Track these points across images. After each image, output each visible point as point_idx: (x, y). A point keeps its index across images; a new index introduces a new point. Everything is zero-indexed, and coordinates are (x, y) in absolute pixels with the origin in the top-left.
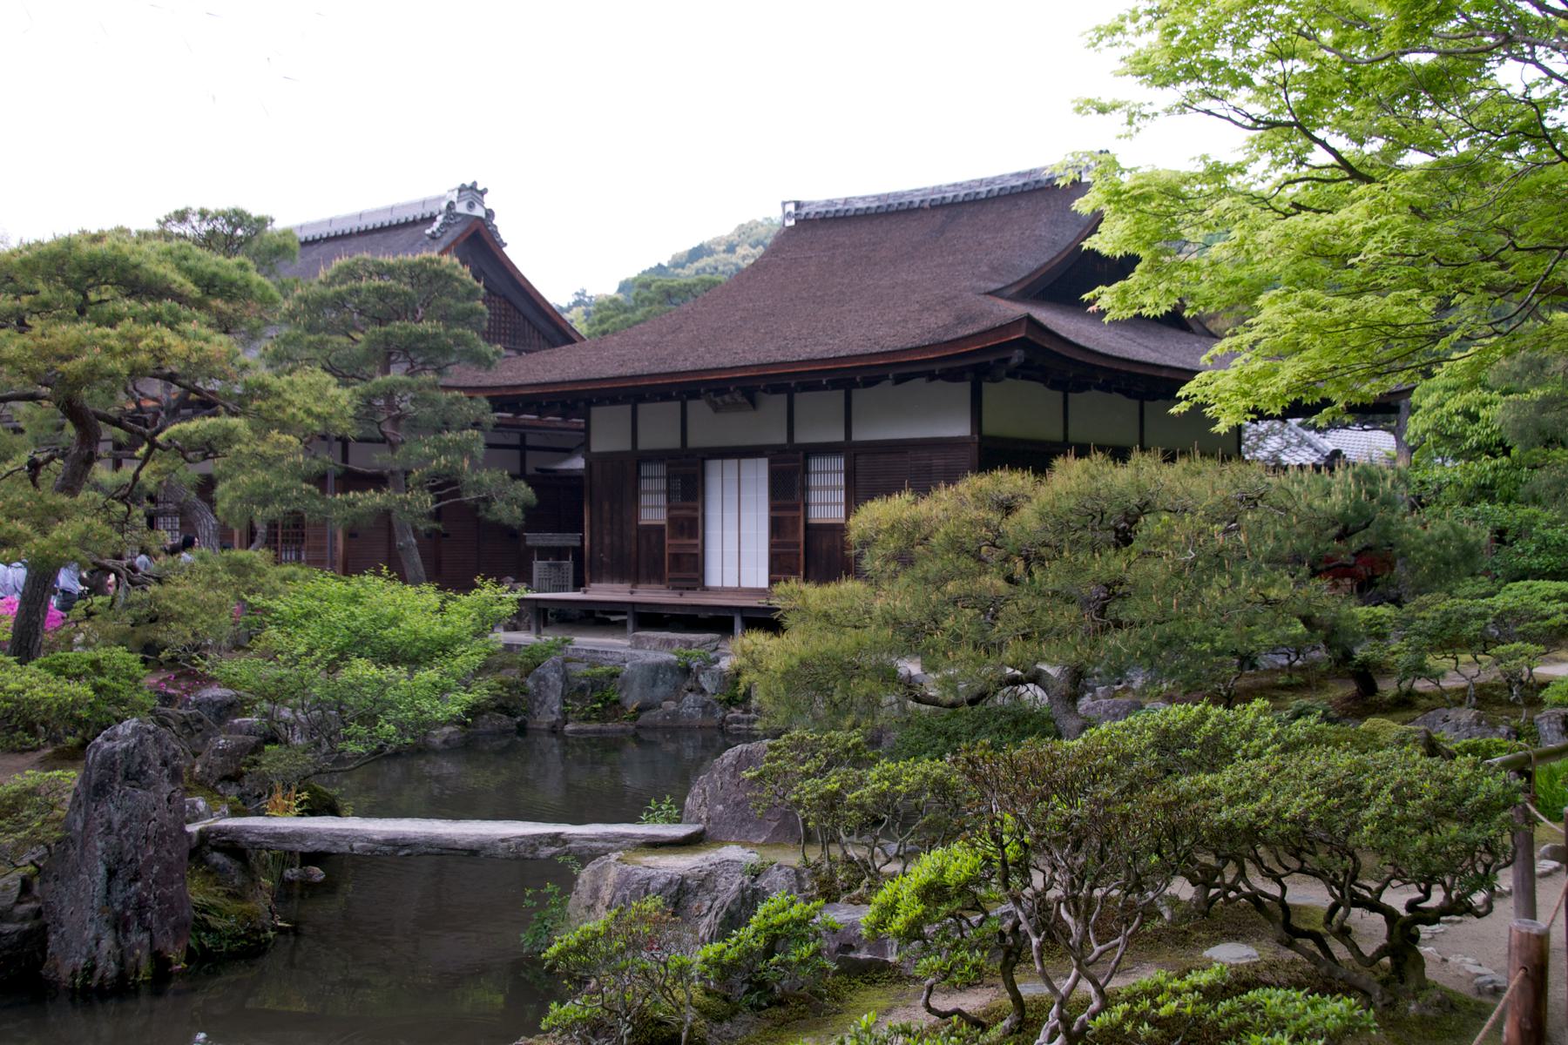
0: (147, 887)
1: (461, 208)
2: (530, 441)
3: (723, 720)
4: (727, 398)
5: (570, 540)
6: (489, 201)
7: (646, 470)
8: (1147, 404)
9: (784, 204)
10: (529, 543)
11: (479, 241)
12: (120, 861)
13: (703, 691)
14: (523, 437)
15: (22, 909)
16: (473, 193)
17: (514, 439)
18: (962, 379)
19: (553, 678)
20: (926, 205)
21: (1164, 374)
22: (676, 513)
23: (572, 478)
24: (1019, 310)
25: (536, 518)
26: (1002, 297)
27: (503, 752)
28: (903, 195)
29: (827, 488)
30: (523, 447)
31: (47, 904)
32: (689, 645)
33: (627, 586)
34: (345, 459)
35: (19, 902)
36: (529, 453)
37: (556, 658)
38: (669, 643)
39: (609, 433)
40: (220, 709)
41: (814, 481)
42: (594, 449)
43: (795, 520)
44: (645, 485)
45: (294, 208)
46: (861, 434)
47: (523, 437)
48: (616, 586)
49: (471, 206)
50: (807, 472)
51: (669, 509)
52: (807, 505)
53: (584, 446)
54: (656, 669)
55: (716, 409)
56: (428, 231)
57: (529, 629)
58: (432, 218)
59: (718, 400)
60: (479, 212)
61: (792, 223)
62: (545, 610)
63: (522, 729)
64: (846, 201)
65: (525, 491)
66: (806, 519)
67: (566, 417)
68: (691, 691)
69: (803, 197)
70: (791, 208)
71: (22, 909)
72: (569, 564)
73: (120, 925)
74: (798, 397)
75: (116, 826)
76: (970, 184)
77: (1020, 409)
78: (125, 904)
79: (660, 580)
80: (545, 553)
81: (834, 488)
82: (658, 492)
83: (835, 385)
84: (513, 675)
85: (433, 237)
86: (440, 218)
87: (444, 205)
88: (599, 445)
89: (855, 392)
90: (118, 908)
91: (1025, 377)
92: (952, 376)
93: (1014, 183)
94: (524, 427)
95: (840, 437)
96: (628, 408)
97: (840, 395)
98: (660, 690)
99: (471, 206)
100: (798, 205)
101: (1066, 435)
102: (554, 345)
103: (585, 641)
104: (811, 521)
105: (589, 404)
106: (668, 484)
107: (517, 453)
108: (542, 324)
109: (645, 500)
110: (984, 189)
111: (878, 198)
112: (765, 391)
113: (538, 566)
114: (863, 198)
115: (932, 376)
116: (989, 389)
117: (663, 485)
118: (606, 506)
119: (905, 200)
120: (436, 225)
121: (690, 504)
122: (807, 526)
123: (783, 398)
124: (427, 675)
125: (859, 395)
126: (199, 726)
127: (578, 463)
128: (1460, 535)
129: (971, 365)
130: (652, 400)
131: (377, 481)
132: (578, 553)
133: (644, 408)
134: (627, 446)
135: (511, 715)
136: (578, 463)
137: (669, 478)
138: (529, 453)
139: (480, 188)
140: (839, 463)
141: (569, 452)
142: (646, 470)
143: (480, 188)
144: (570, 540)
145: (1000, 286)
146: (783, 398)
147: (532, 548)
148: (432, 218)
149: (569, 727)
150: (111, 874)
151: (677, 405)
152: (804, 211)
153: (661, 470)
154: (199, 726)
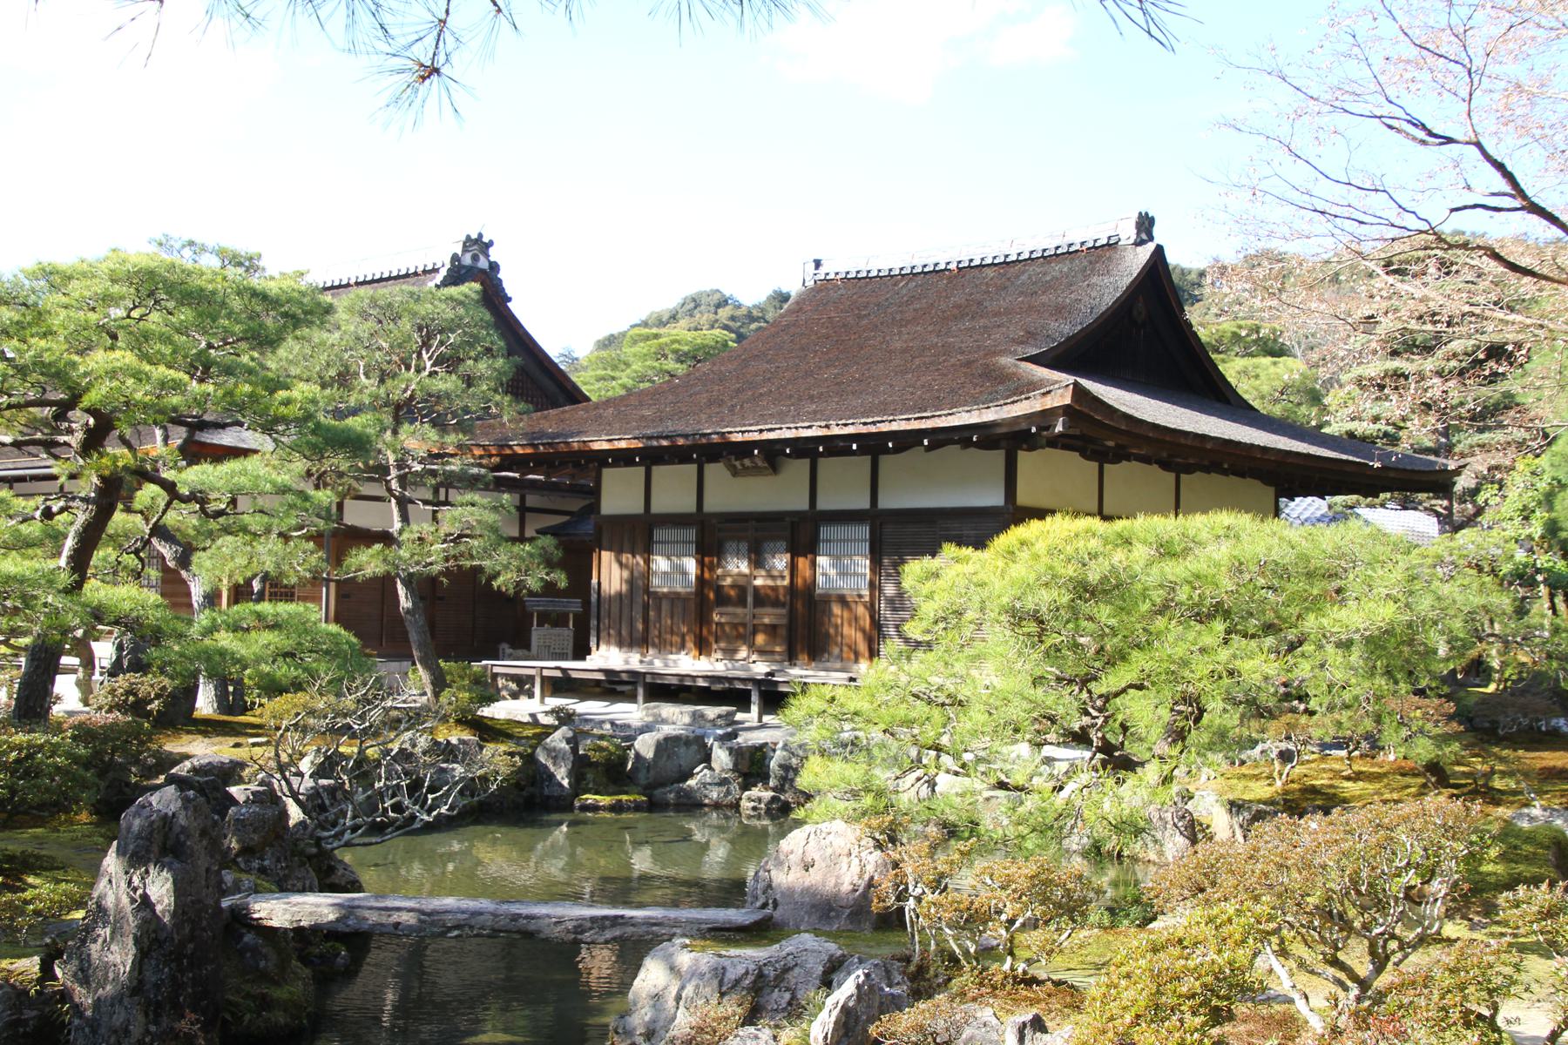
1: (467, 260)
4: (747, 462)
6: (494, 254)
20: (953, 266)
46: (887, 502)
55: (735, 473)
58: (435, 270)
59: (737, 463)
60: (483, 264)
74: (822, 462)
83: (862, 451)
86: (443, 272)
95: (864, 503)
99: (475, 258)
102: (555, 405)
108: (546, 382)
113: (537, 635)
115: (966, 443)
116: (1025, 459)
123: (806, 462)
125: (886, 462)
128: (1557, 680)
130: (615, 464)
133: (658, 471)
139: (485, 240)
140: (864, 531)
143: (485, 240)
146: (806, 462)
148: (435, 270)
151: (694, 467)
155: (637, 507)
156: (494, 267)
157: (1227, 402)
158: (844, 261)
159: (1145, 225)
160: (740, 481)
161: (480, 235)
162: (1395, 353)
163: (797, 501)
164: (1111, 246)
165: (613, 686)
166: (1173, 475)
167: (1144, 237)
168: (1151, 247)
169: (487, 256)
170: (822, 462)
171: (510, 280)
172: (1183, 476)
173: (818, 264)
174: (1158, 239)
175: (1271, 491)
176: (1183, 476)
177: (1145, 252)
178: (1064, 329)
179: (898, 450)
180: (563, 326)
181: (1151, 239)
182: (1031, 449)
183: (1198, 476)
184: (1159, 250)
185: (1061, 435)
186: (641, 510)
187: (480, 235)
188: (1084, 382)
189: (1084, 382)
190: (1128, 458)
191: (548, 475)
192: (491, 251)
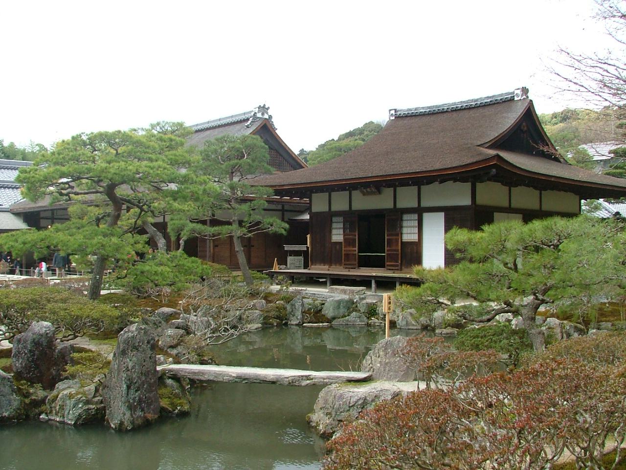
1: (259, 115)
2: (286, 208)
4: (368, 190)
5: (303, 248)
6: (270, 112)
7: (334, 219)
9: (390, 110)
10: (285, 249)
14: (283, 206)
16: (264, 109)
17: (280, 207)
20: (449, 110)
22: (347, 237)
26: (483, 147)
28: (440, 106)
30: (283, 211)
32: (353, 292)
33: (327, 267)
36: (285, 213)
38: (345, 292)
39: (319, 204)
40: (167, 316)
41: (405, 224)
43: (397, 241)
44: (334, 225)
45: (192, 119)
47: (283, 206)
48: (322, 267)
49: (263, 114)
50: (402, 220)
51: (344, 236)
52: (402, 234)
53: (308, 209)
55: (364, 195)
56: (246, 124)
58: (248, 119)
59: (365, 190)
60: (266, 116)
61: (394, 118)
62: (293, 277)
63: (286, 324)
64: (416, 109)
66: (401, 240)
67: (301, 198)
69: (398, 108)
70: (393, 112)
74: (398, 189)
76: (467, 102)
77: (491, 193)
79: (340, 264)
81: (413, 227)
82: (340, 228)
83: (414, 184)
85: (248, 127)
87: (252, 114)
88: (315, 209)
89: (422, 187)
94: (284, 202)
95: (416, 205)
97: (415, 189)
99: (263, 114)
100: (395, 110)
101: (510, 205)
104: (403, 241)
105: (312, 192)
106: (344, 225)
109: (334, 232)
110: (474, 103)
111: (429, 107)
112: (385, 187)
113: (290, 259)
114: (423, 108)
115: (455, 180)
117: (341, 225)
120: (250, 122)
121: (353, 233)
122: (402, 242)
126: (160, 325)
132: (305, 254)
133: (333, 194)
136: (307, 217)
139: (266, 107)
141: (302, 212)
142: (334, 219)
143: (266, 107)
148: (248, 119)
152: (398, 113)
153: (341, 219)
154: (160, 325)
155: (326, 209)
156: (270, 117)
163: (389, 205)
164: (512, 100)
166: (538, 192)
169: (267, 113)
172: (543, 192)
174: (530, 98)
175: (577, 197)
176: (543, 192)
179: (428, 183)
181: (528, 97)
183: (549, 191)
185: (493, 176)
188: (503, 154)
189: (503, 154)
191: (291, 198)
192: (269, 111)
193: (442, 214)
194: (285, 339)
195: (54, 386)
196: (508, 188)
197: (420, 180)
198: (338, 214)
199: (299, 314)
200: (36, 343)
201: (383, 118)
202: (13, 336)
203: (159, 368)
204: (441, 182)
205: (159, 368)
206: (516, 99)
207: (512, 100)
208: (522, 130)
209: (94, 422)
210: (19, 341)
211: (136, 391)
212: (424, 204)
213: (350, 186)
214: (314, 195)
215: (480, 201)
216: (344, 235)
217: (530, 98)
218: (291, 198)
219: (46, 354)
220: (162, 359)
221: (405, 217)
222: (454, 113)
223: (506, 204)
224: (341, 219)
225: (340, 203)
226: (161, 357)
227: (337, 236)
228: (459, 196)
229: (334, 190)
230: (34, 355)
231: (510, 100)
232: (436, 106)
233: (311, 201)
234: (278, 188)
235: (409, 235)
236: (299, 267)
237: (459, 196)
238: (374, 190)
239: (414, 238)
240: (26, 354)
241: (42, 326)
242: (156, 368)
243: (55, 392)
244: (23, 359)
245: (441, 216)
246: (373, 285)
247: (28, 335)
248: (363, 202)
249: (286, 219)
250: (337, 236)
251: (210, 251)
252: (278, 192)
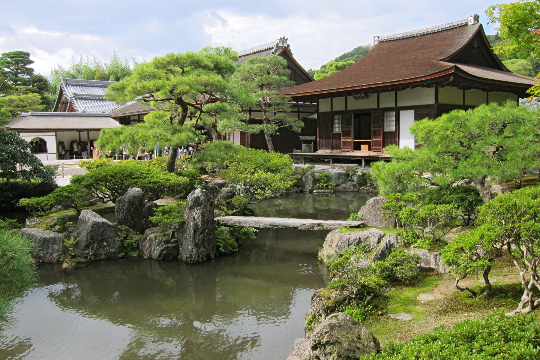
0: (204, 236)
1: (280, 44)
2: (301, 110)
3: (359, 189)
4: (359, 95)
5: (313, 138)
7: (335, 117)
8: (489, 93)
9: (375, 37)
11: (286, 53)
12: (197, 228)
13: (353, 181)
15: (172, 240)
16: (284, 40)
17: (296, 110)
18: (433, 87)
19: (310, 177)
21: (497, 83)
23: (314, 120)
24: (452, 65)
25: (305, 132)
27: (296, 198)
29: (390, 121)
30: (298, 112)
31: (179, 239)
34: (250, 116)
35: (172, 238)
36: (300, 114)
37: (310, 172)
39: (324, 106)
41: (386, 119)
42: (321, 110)
43: (380, 131)
44: (335, 121)
49: (283, 44)
50: (383, 116)
52: (383, 126)
53: (317, 111)
54: (340, 175)
55: (356, 98)
57: (302, 163)
58: (272, 48)
60: (285, 45)
63: (301, 191)
65: (302, 124)
68: (349, 181)
70: (377, 38)
71: (172, 240)
72: (312, 145)
73: (197, 245)
74: (381, 94)
75: (196, 218)
77: (449, 95)
78: (199, 240)
80: (306, 142)
81: (392, 121)
82: (339, 123)
83: (392, 90)
84: (299, 177)
86: (275, 48)
87: (276, 44)
90: (197, 241)
91: (453, 86)
92: (428, 86)
93: (446, 26)
95: (394, 106)
96: (330, 99)
98: (341, 181)
99: (283, 44)
103: (318, 167)
107: (297, 114)
108: (303, 77)
109: (335, 126)
112: (371, 93)
113: (304, 146)
114: (399, 34)
118: (324, 128)
119: (412, 34)
120: (274, 50)
122: (384, 133)
124: (278, 176)
127: (316, 116)
129: (437, 82)
131: (260, 122)
133: (334, 99)
134: (329, 110)
135: (298, 187)
136: (316, 116)
137: (342, 119)
138: (300, 114)
141: (312, 113)
142: (335, 117)
144: (313, 138)
145: (444, 58)
147: (302, 140)
148: (272, 48)
149: (314, 191)
150: (195, 232)
152: (380, 39)
153: (340, 117)
155: (329, 110)
156: (288, 46)
157: (502, 70)
158: (385, 35)
159: (476, 18)
160: (357, 101)
161: (284, 37)
162: (158, 68)
164: (466, 25)
165: (322, 160)
167: (476, 22)
168: (478, 25)
169: (286, 43)
170: (380, 94)
171: (293, 50)
173: (378, 37)
174: (480, 23)
177: (477, 27)
178: (452, 51)
179: (403, 89)
180: (309, 62)
181: (478, 22)
182: (443, 87)
184: (481, 25)
185: (451, 82)
186: (344, 109)
187: (284, 37)
188: (459, 66)
189: (459, 66)
190: (472, 88)
193: (412, 112)
194: (301, 203)
195: (144, 232)
196: (462, 91)
197: (396, 88)
198: (338, 113)
199: (310, 182)
200: (131, 202)
201: (370, 42)
202: (115, 199)
203: (215, 219)
204: (413, 88)
205: (215, 219)
206: (469, 24)
207: (466, 25)
208: (473, 48)
209: (170, 257)
210: (120, 201)
211: (201, 234)
212: (400, 105)
213: (346, 94)
214: (320, 100)
215: (440, 101)
216: (342, 128)
217: (480, 23)
218: (304, 102)
219: (138, 210)
220: (218, 212)
221: (386, 114)
222: (423, 37)
223: (461, 103)
224: (340, 117)
225: (339, 104)
226: (216, 211)
227: (337, 129)
228: (427, 98)
229: (335, 96)
230: (130, 211)
231: (465, 25)
232: (409, 33)
233: (318, 104)
234: (295, 96)
235: (389, 126)
236: (310, 152)
237: (427, 98)
238: (363, 95)
239: (392, 129)
240: (124, 210)
241: (135, 191)
242: (213, 219)
243: (144, 236)
244: (123, 213)
245: (412, 112)
246: (363, 163)
247: (126, 197)
248: (355, 104)
249: (301, 118)
250: (337, 129)
251: (248, 141)
252: (294, 99)
